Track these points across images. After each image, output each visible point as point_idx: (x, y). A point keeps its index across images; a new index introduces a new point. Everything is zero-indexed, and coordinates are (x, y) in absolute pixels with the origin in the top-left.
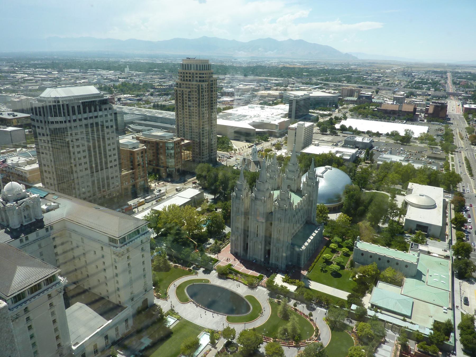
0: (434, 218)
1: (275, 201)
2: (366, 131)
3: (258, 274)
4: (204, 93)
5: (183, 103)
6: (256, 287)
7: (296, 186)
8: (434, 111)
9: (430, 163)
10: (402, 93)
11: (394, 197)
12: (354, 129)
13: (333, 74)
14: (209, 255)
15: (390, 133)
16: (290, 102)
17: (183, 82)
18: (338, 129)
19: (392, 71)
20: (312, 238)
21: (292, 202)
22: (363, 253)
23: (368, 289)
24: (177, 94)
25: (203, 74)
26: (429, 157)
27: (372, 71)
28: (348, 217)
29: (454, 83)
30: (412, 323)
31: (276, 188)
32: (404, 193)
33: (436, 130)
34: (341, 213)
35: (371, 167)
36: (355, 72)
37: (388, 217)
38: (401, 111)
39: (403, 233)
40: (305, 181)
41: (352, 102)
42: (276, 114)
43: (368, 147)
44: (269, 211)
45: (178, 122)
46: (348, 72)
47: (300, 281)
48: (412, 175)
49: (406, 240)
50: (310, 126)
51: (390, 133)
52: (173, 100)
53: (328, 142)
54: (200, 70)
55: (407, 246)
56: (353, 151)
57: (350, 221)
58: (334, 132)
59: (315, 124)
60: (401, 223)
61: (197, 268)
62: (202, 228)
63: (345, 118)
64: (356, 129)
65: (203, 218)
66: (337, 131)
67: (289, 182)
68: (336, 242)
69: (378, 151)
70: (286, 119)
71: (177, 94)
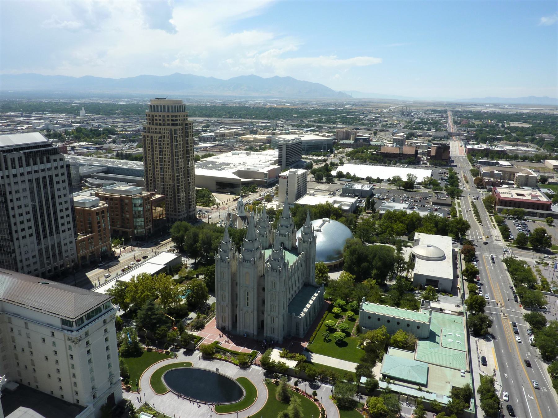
0: (443, 271)
1: (267, 262)
2: (365, 177)
3: (250, 351)
4: (178, 139)
5: (153, 151)
6: (249, 367)
7: (290, 243)
8: (436, 153)
9: (436, 210)
10: (402, 134)
11: (400, 250)
12: (352, 175)
13: (326, 115)
14: (190, 333)
15: (391, 179)
16: (280, 147)
17: (153, 126)
18: (335, 177)
19: (390, 110)
20: (311, 302)
21: (286, 261)
22: (370, 316)
23: (378, 357)
24: (145, 140)
25: (176, 116)
26: (434, 203)
27: (369, 110)
28: (351, 275)
29: (455, 123)
30: (428, 392)
31: (267, 247)
32: (411, 244)
33: (440, 173)
34: (342, 272)
35: (373, 217)
36: (351, 112)
37: (395, 273)
38: (402, 154)
39: (412, 290)
40: (300, 236)
41: (348, 146)
42: (264, 161)
43: (369, 195)
44: (260, 274)
45: (147, 174)
46: (342, 112)
47: (300, 355)
48: (418, 224)
49: (416, 298)
50: (303, 174)
51: (391, 179)
52: (140, 147)
53: (324, 191)
54: (172, 112)
55: (417, 304)
56: (353, 200)
57: (353, 280)
58: (330, 180)
59: (309, 171)
60: (409, 279)
61: (177, 349)
62: (180, 300)
63: (342, 164)
64: (354, 175)
65: (181, 288)
66: (334, 179)
67: (282, 239)
68: (340, 306)
69: (379, 199)
70: (276, 167)
71: (145, 140)
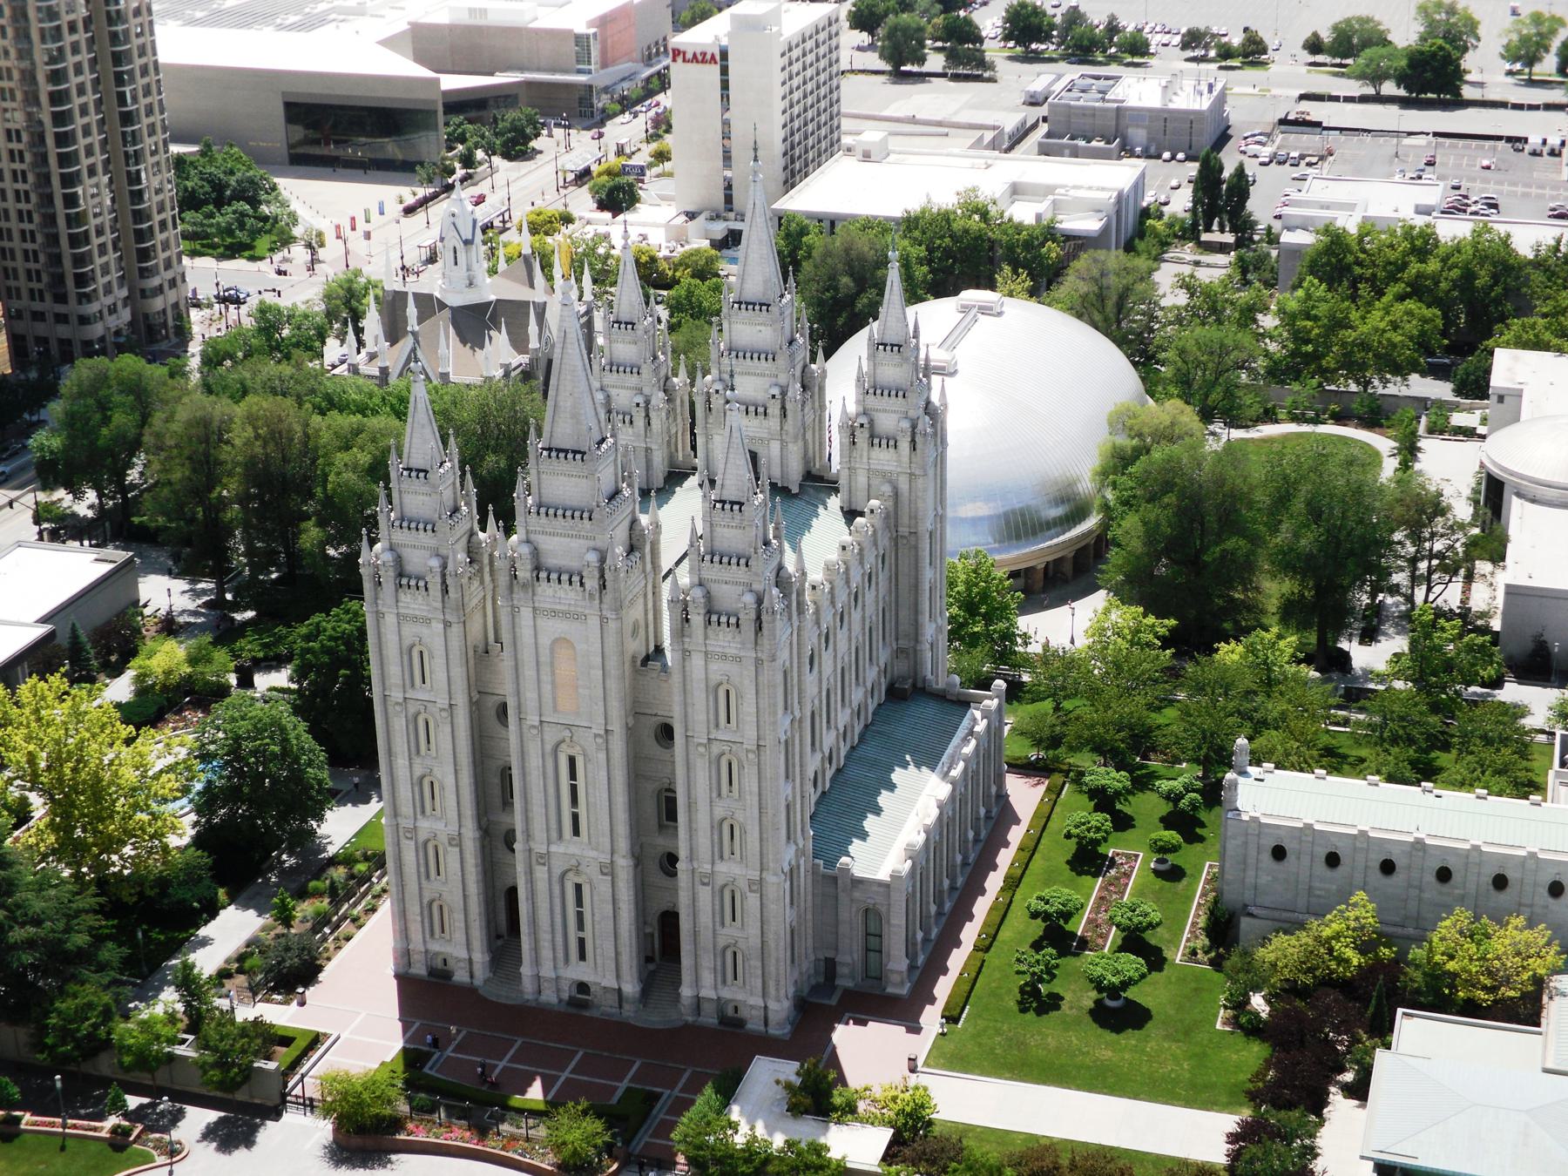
28: (1151, 620)
35: (1243, 267)
